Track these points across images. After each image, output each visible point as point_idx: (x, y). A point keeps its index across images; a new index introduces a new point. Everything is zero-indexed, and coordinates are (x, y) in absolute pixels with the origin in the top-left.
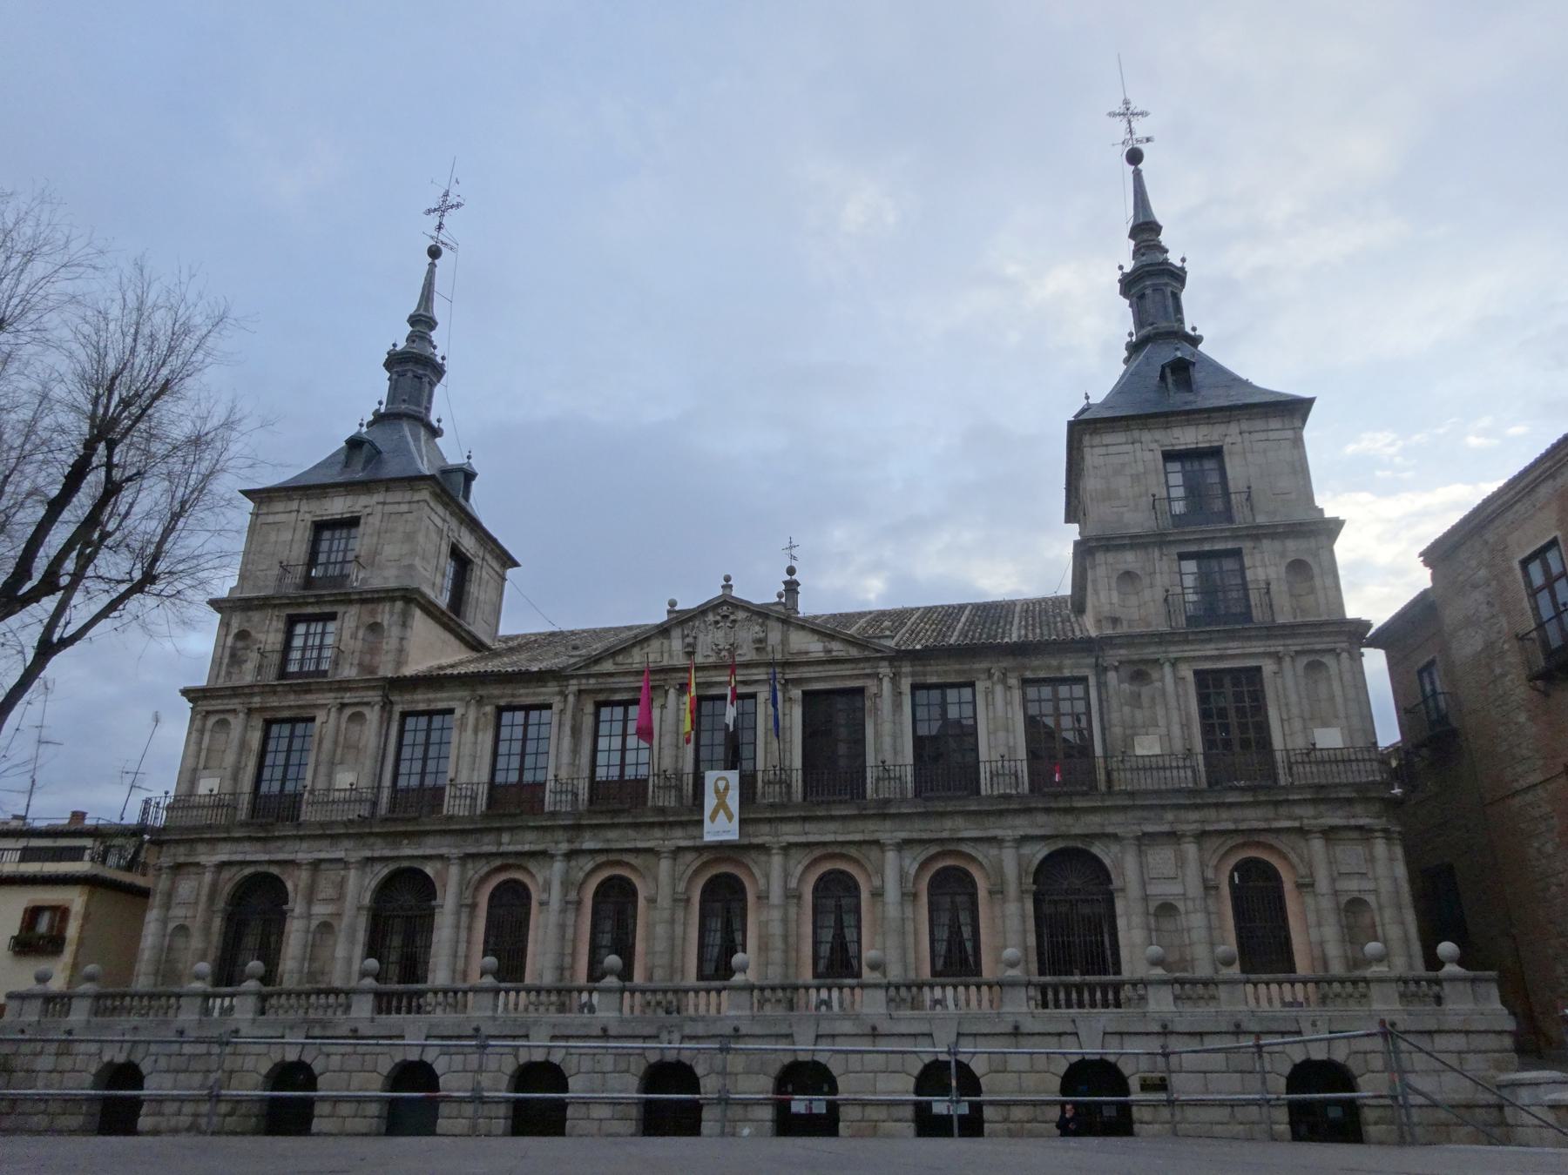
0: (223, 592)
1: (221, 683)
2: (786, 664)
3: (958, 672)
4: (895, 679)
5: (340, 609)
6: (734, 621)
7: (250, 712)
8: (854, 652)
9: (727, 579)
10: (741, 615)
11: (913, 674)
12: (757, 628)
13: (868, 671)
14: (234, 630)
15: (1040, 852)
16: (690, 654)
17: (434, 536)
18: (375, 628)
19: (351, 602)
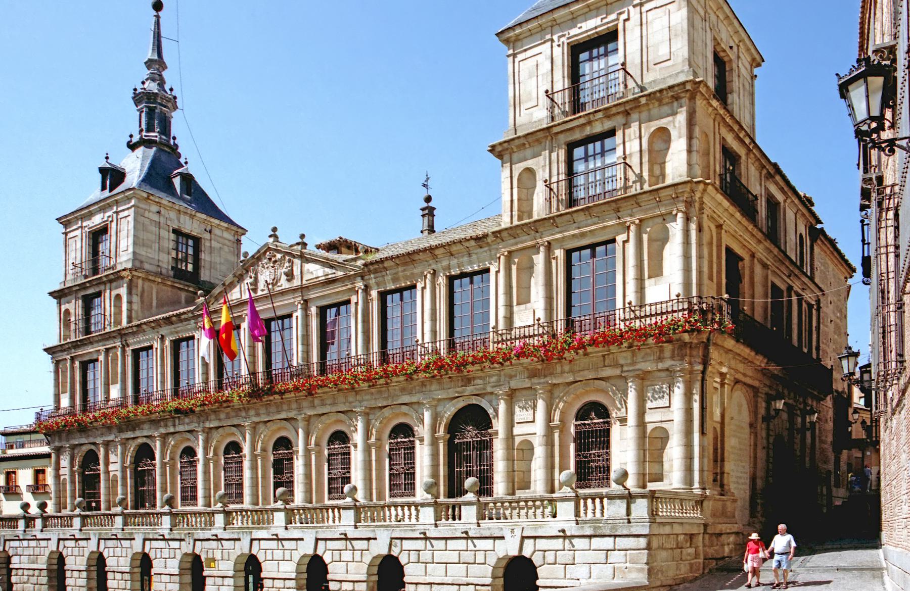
0: (57, 287)
1: (63, 342)
2: (302, 289)
3: (406, 278)
4: (367, 289)
5: (102, 287)
6: (275, 262)
7: (73, 359)
8: (340, 274)
9: (275, 229)
10: (279, 256)
11: (378, 284)
12: (287, 264)
13: (350, 286)
14: (63, 310)
15: (449, 411)
16: (255, 290)
17: (154, 229)
18: (118, 297)
19: (104, 283)
